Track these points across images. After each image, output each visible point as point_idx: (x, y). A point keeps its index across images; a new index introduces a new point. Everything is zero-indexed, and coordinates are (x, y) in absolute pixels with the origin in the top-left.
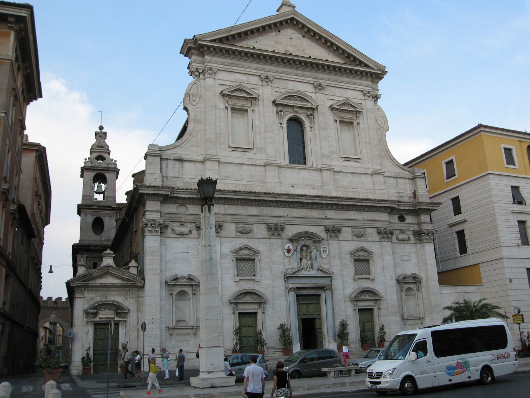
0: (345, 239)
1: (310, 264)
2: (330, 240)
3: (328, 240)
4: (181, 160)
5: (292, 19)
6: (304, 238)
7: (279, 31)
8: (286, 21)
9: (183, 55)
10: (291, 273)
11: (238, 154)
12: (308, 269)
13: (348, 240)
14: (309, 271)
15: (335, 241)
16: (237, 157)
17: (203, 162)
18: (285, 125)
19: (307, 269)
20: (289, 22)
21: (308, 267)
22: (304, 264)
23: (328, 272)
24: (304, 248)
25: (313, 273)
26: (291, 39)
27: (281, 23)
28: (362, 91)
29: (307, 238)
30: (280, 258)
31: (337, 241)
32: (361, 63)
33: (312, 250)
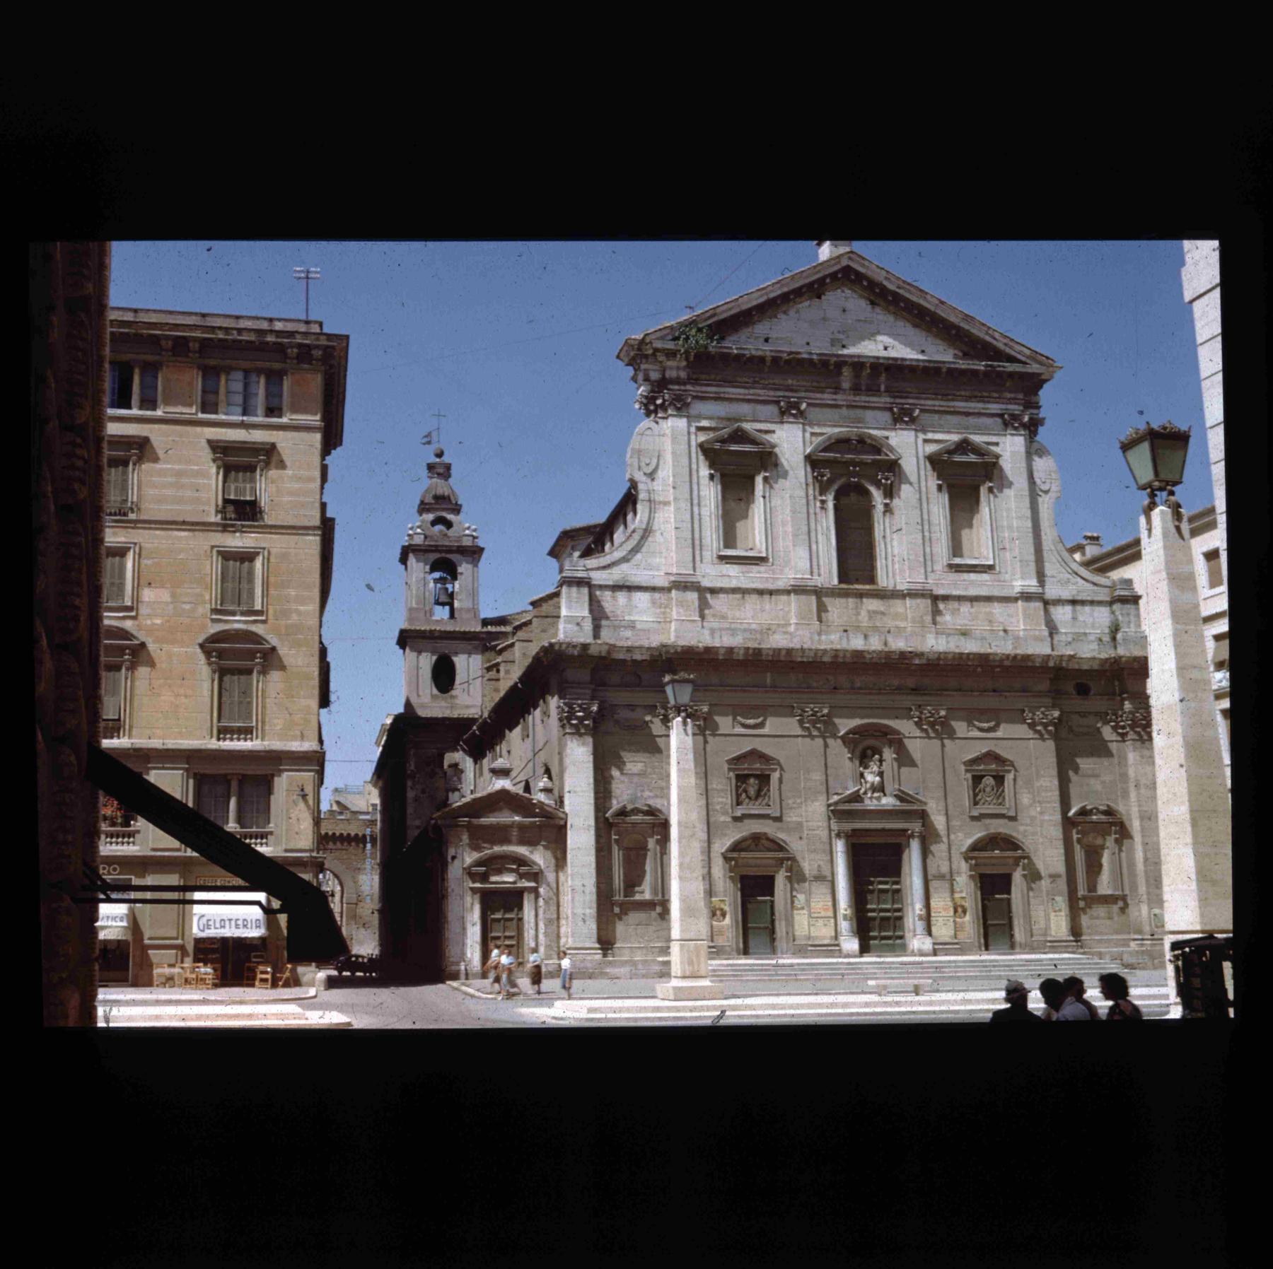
4: (630, 588)
5: (847, 270)
7: (819, 297)
8: (833, 276)
9: (620, 363)
11: (733, 570)
16: (734, 575)
17: (669, 590)
18: (830, 505)
20: (840, 276)
24: (869, 752)
25: (888, 802)
26: (844, 311)
27: (822, 281)
28: (1001, 416)
32: (999, 355)
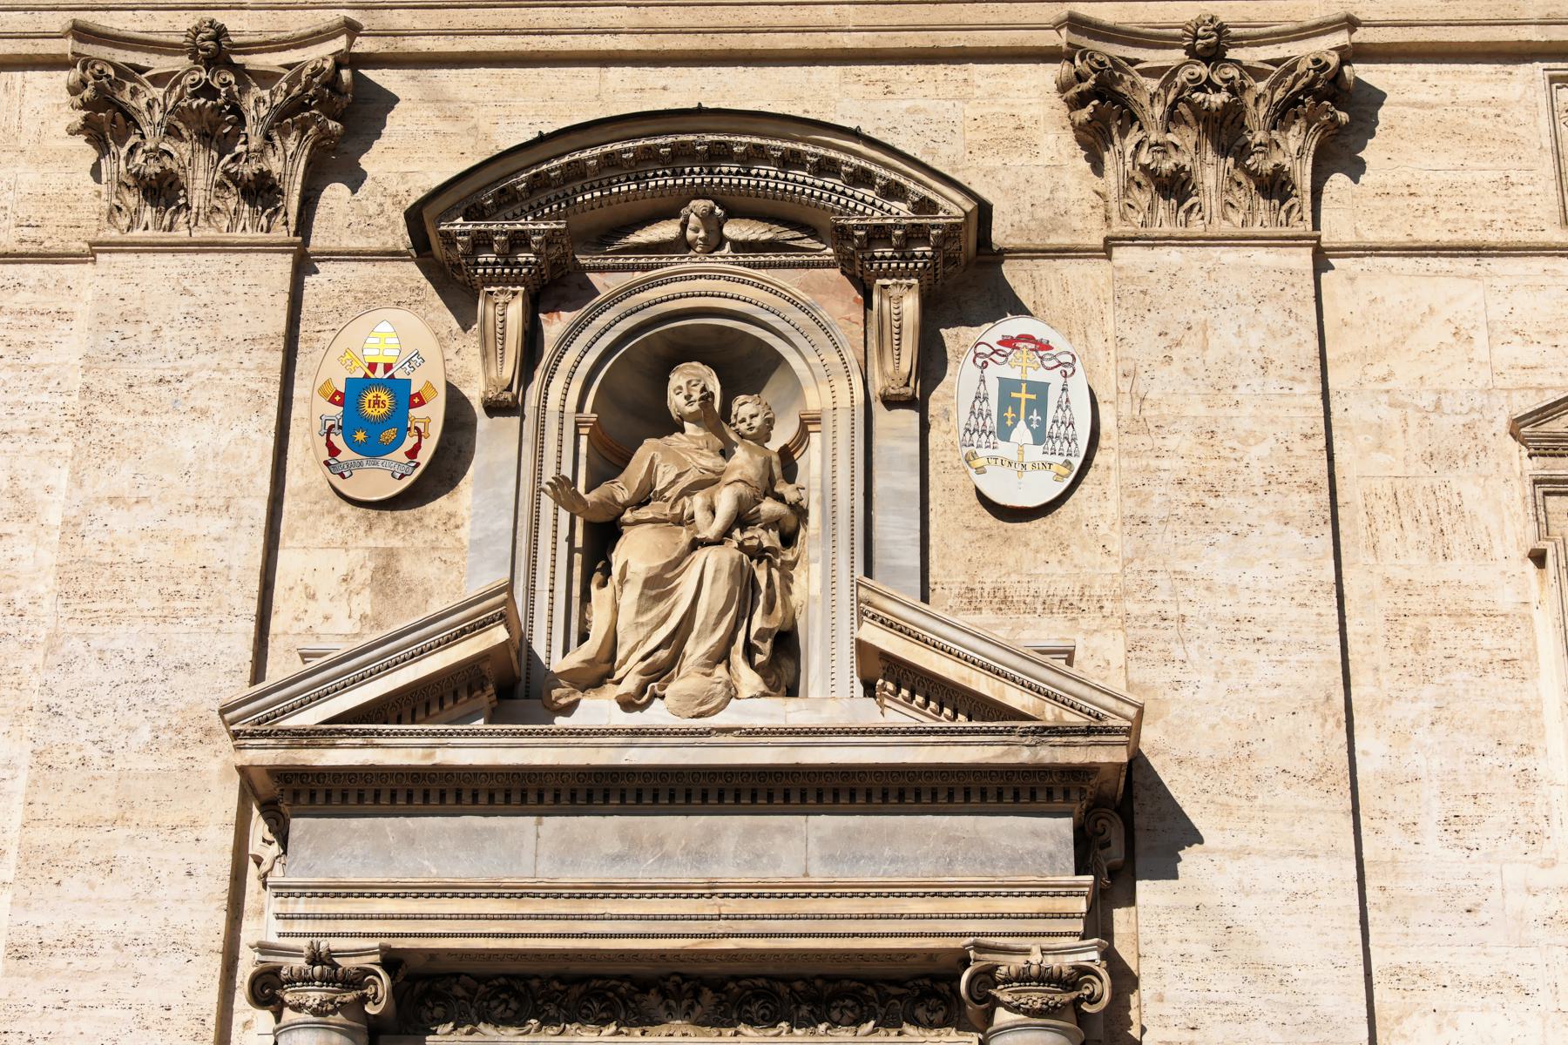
0: (1429, 233)
1: (715, 595)
2: (1153, 242)
3: (1108, 248)
6: (666, 231)
10: (309, 718)
12: (687, 681)
13: (1492, 237)
14: (704, 706)
15: (1229, 255)
19: (660, 672)
21: (696, 649)
22: (630, 596)
23: (1015, 698)
29: (736, 230)
30: (218, 525)
31: (1262, 256)
33: (815, 399)
